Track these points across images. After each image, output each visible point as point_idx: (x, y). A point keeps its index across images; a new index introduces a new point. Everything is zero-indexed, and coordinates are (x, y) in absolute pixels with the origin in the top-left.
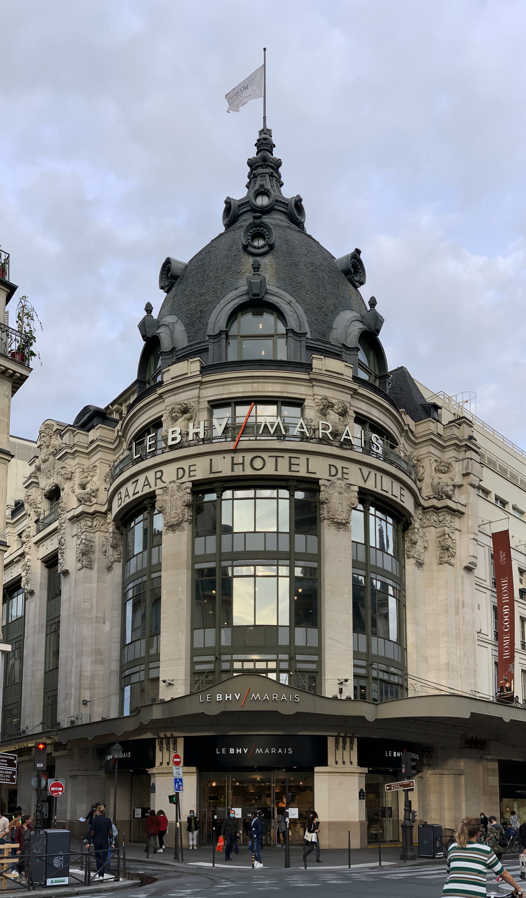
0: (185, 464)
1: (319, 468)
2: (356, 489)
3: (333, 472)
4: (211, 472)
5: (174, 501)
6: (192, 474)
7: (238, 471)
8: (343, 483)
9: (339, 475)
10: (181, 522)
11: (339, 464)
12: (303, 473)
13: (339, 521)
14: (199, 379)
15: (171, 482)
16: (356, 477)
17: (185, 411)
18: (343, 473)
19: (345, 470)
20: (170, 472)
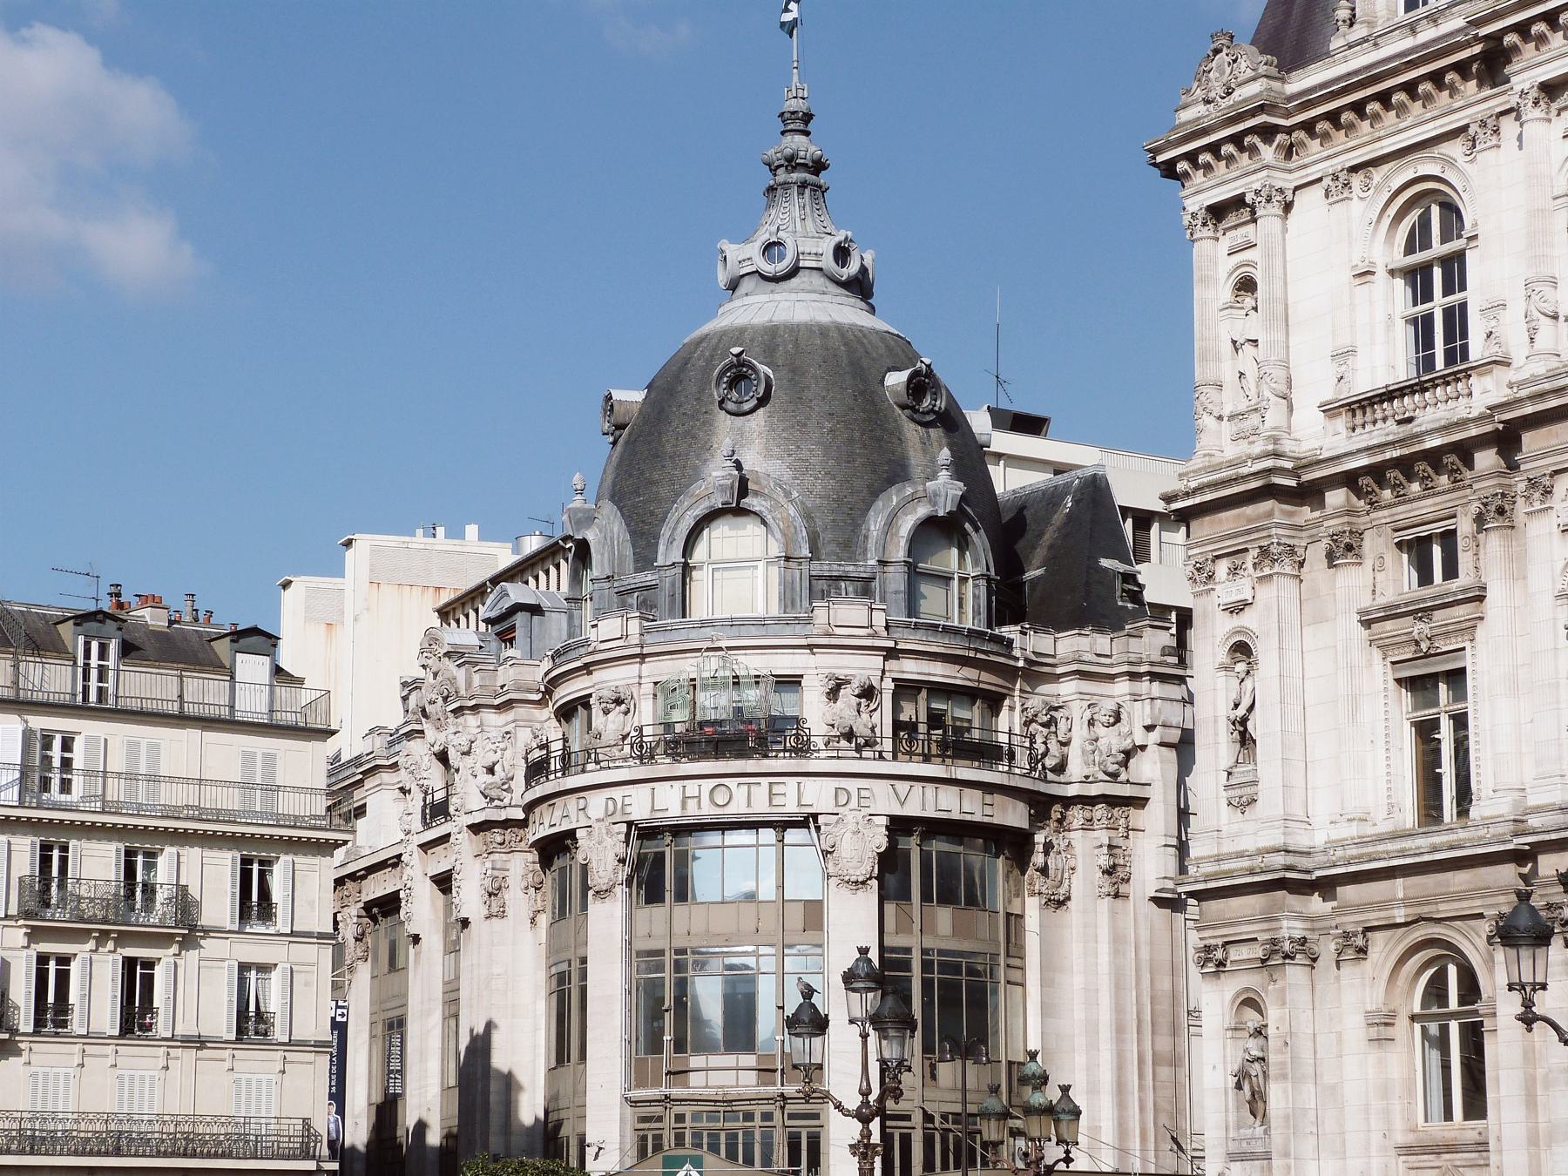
0: (617, 793)
1: (818, 795)
2: (884, 821)
3: (843, 799)
4: (653, 810)
5: (603, 853)
6: (628, 809)
7: (692, 809)
8: (860, 815)
9: (854, 803)
10: (613, 886)
11: (852, 785)
12: (789, 806)
13: (853, 879)
14: (637, 651)
15: (598, 820)
16: (887, 801)
17: (619, 702)
18: (860, 797)
19: (863, 793)
20: (597, 803)
